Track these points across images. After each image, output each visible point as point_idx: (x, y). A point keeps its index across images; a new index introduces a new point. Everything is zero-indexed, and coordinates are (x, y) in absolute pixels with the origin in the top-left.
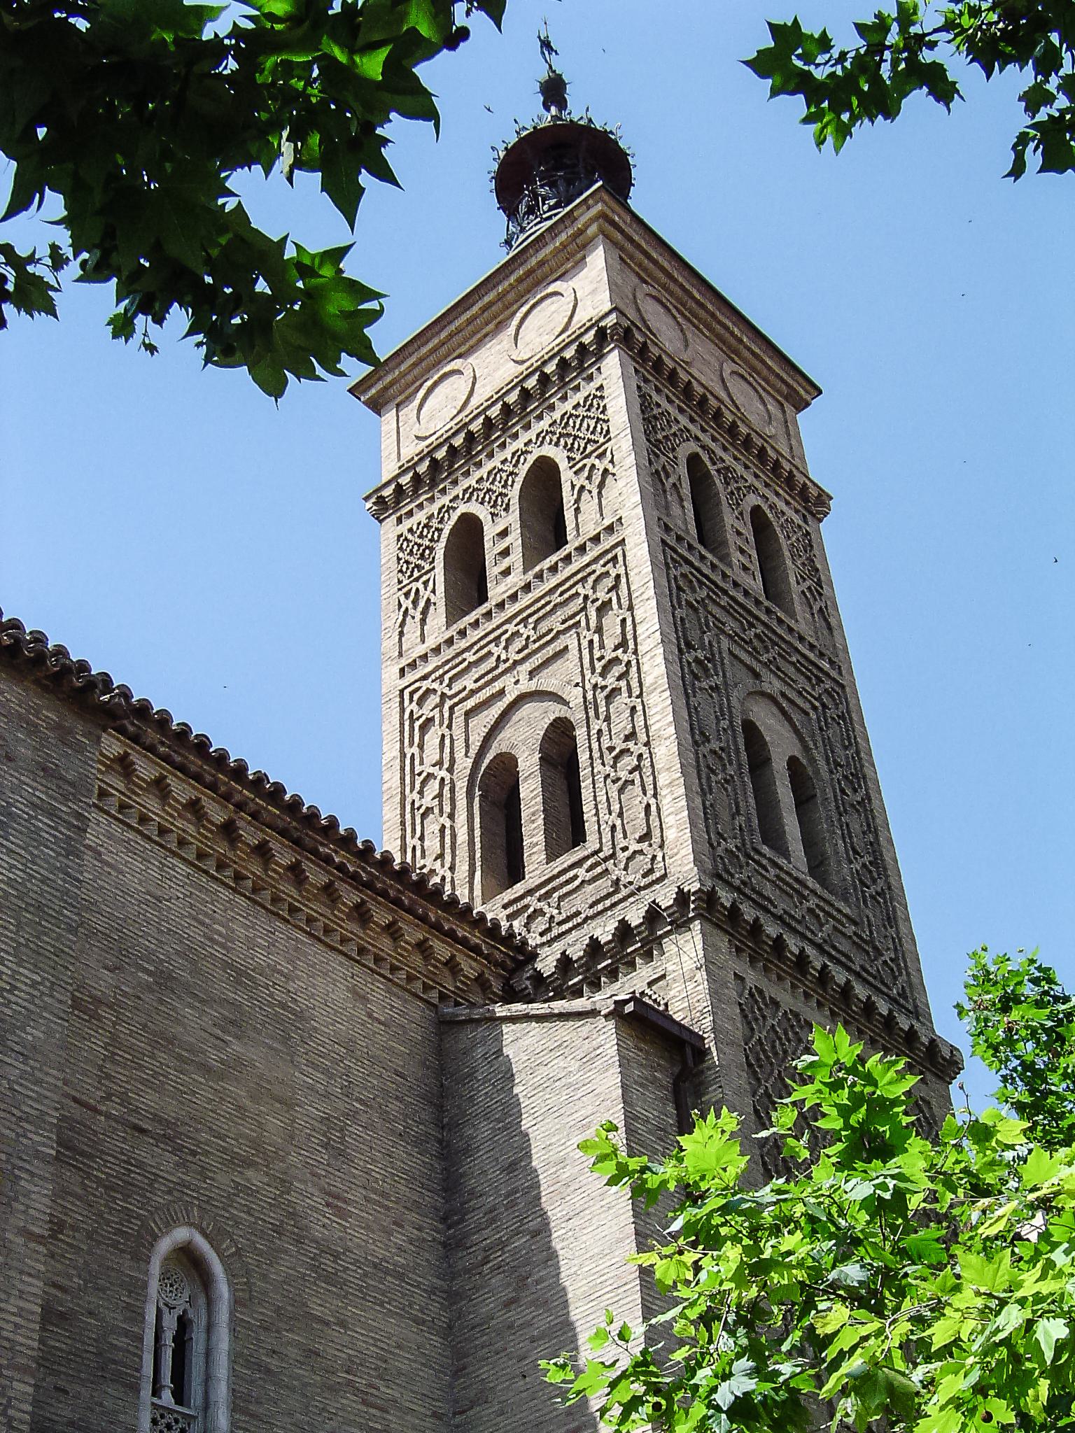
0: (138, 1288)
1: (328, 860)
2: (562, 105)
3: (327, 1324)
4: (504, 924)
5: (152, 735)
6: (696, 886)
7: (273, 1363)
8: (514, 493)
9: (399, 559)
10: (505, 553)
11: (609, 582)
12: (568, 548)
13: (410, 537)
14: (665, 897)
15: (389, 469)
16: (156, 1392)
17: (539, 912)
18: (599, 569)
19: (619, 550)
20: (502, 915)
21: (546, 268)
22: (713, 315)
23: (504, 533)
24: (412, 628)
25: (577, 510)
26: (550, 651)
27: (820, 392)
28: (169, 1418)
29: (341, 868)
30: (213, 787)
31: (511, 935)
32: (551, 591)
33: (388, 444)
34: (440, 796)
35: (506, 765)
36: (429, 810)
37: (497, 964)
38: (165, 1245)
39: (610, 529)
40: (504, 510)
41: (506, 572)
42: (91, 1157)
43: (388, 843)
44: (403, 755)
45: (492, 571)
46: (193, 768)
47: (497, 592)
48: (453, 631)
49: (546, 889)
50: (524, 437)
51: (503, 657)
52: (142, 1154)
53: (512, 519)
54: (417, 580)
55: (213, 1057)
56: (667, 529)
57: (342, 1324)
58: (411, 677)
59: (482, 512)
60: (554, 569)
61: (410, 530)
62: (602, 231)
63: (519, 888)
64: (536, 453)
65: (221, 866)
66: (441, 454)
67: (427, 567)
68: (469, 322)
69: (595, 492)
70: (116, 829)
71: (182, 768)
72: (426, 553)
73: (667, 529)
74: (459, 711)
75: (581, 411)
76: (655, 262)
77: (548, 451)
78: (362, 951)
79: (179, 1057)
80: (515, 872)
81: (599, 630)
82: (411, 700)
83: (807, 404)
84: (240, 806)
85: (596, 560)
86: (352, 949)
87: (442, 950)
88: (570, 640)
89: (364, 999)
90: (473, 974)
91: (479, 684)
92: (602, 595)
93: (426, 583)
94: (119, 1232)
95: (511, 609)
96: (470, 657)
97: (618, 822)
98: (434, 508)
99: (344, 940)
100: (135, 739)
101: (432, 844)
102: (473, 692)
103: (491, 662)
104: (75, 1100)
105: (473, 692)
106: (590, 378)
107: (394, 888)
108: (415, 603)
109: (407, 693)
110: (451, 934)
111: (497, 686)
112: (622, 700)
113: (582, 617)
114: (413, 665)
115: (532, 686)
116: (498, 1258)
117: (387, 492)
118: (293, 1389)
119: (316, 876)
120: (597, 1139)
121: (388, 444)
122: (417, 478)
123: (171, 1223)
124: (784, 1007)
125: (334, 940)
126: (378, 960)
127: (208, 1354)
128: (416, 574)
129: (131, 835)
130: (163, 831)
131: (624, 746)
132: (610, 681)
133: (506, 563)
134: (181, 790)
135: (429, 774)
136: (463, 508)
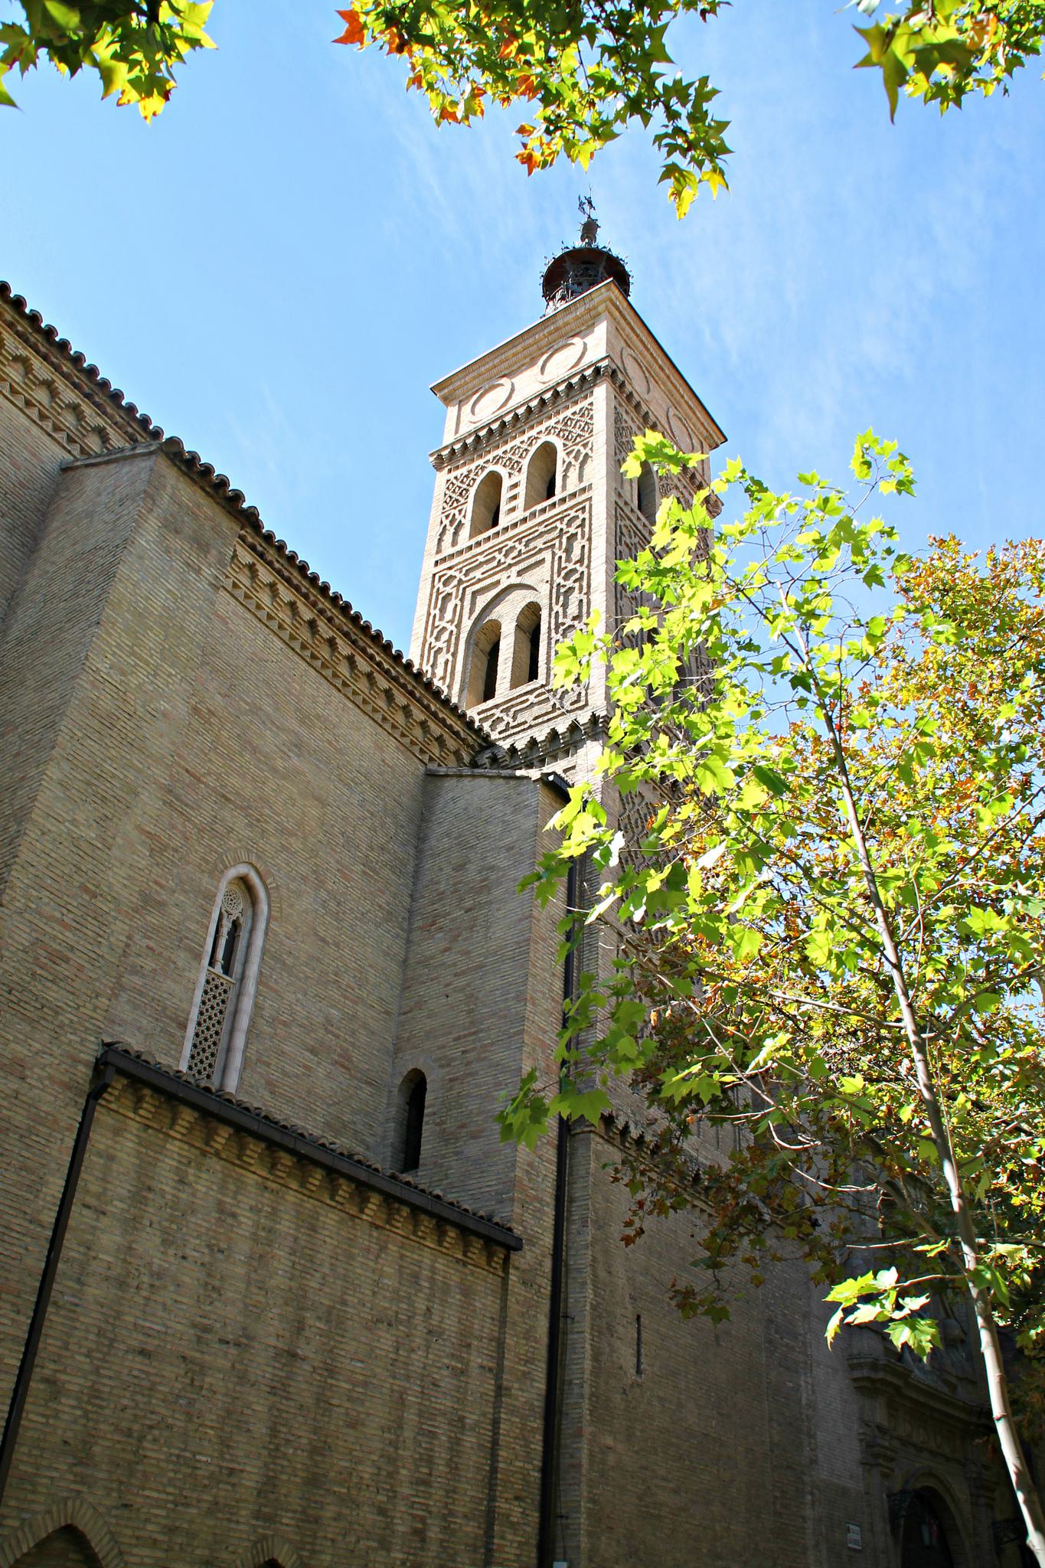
0: (210, 898)
1: (372, 658)
2: (593, 238)
3: (327, 943)
4: (477, 724)
5: (271, 554)
6: (604, 713)
7: (289, 961)
8: (525, 463)
10: (514, 497)
11: (578, 522)
14: (583, 718)
15: (449, 438)
16: (211, 963)
17: (500, 719)
18: (572, 513)
19: (587, 504)
20: (477, 718)
23: (515, 485)
24: (448, 537)
26: (532, 560)
28: (218, 982)
29: (379, 664)
30: (306, 596)
31: (481, 729)
32: (540, 524)
33: (450, 424)
34: (449, 641)
35: (496, 626)
36: (440, 650)
37: (468, 746)
38: (232, 873)
39: (583, 490)
41: (513, 509)
42: (192, 808)
43: (412, 653)
44: (429, 614)
45: (504, 507)
46: (295, 582)
47: (504, 520)
48: (473, 542)
49: (507, 706)
50: (537, 429)
52: (226, 814)
53: (522, 477)
55: (279, 764)
56: (620, 495)
57: (337, 945)
58: (441, 567)
59: (503, 472)
60: (544, 511)
63: (490, 703)
64: (543, 438)
65: (304, 647)
66: (482, 433)
68: (514, 355)
70: (241, 609)
71: (288, 580)
73: (620, 495)
74: (469, 591)
75: (577, 417)
76: (638, 336)
77: (552, 439)
78: (384, 719)
79: (259, 760)
80: (489, 692)
83: (717, 446)
84: (322, 612)
85: (571, 508)
86: (378, 717)
87: (436, 729)
88: (547, 555)
89: (381, 749)
90: (452, 749)
92: (572, 530)
94: (203, 859)
95: (511, 533)
96: (481, 559)
98: (473, 466)
99: (375, 710)
100: (261, 556)
101: (439, 672)
102: (480, 580)
103: (495, 563)
104: (187, 771)
105: (480, 580)
106: (586, 397)
107: (411, 684)
108: (452, 523)
110: (443, 721)
113: (557, 542)
114: (444, 560)
116: (441, 922)
117: (445, 453)
118: (299, 979)
119: (363, 665)
121: (450, 424)
122: (465, 446)
123: (238, 861)
124: (646, 800)
125: (368, 709)
126: (394, 727)
127: (249, 946)
129: (248, 616)
130: (270, 617)
132: (569, 583)
134: (286, 594)
136: (491, 468)
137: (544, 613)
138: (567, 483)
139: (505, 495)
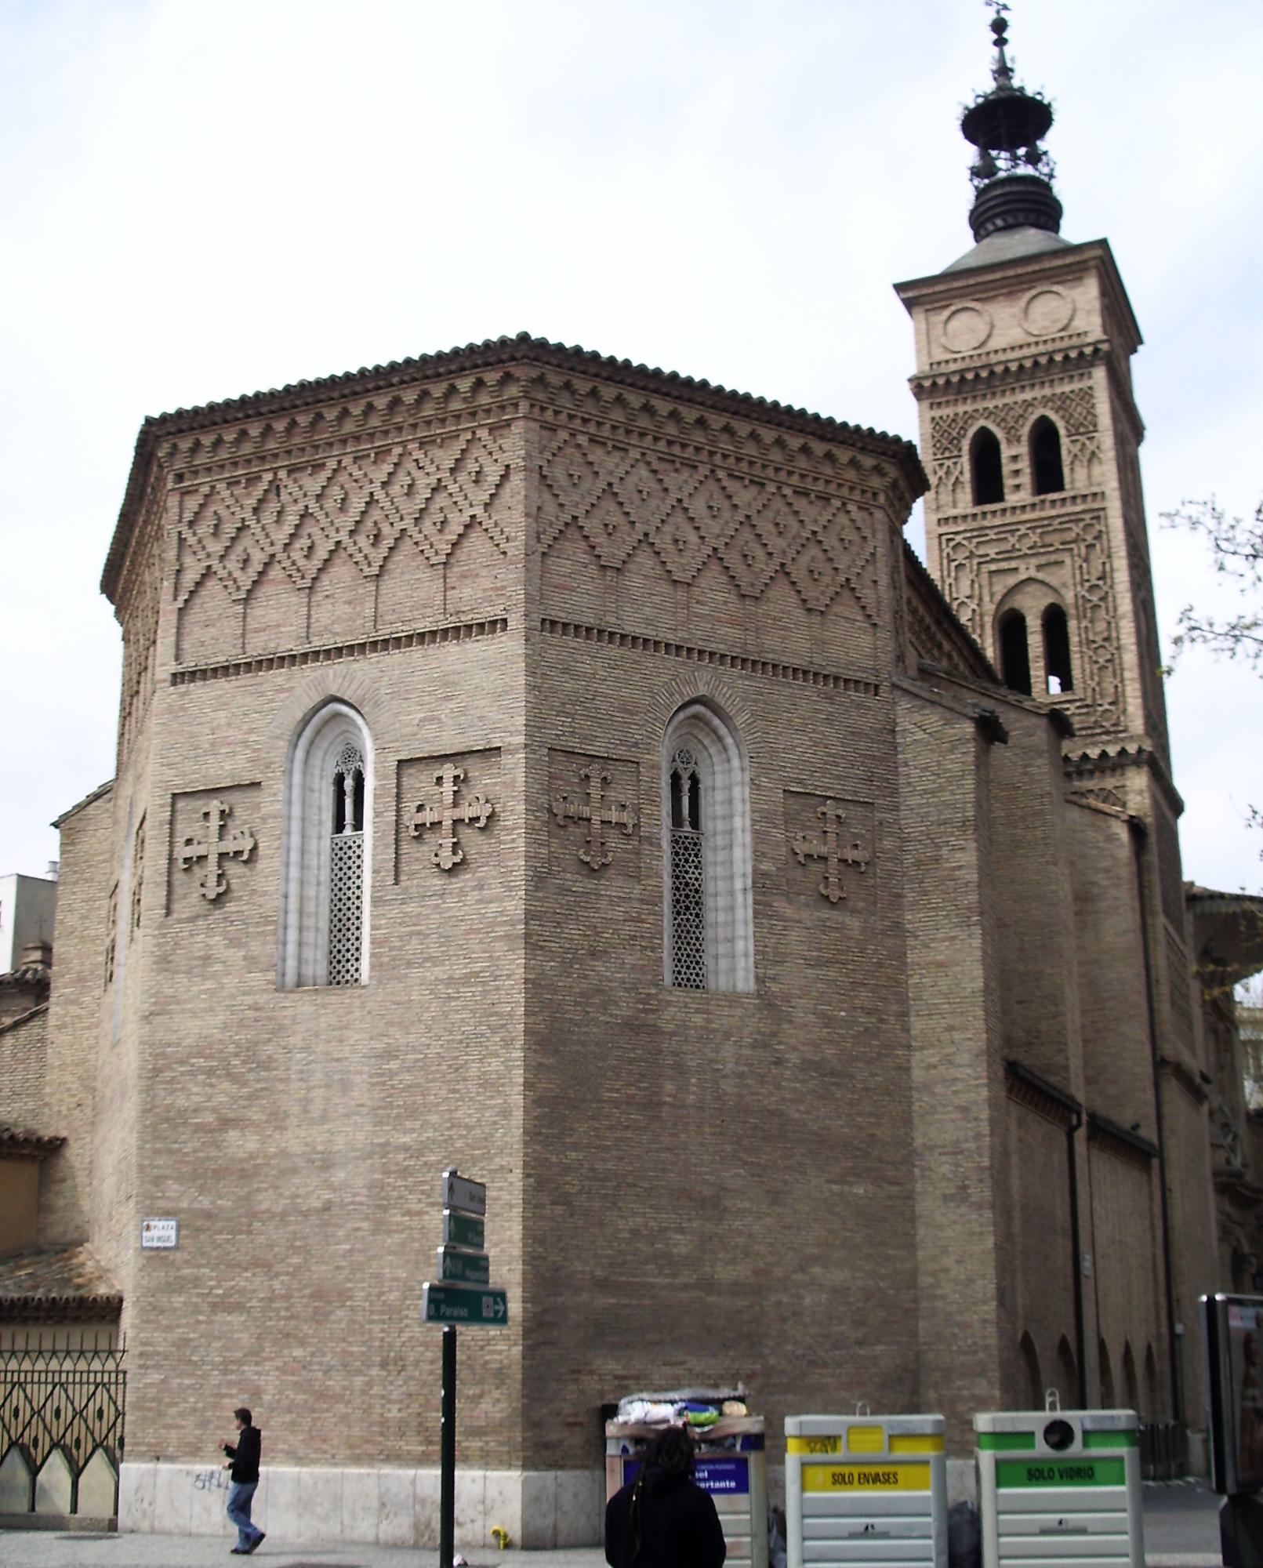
9: (933, 437)
13: (941, 423)
25: (1072, 470)
45: (1009, 482)
51: (1017, 546)
53: (1023, 449)
54: (948, 458)
61: (941, 418)
67: (956, 453)
69: (1086, 464)
72: (955, 441)
81: (1086, 560)
82: (947, 546)
91: (1000, 556)
93: (955, 463)
97: (1097, 688)
109: (944, 538)
111: (1013, 564)
112: (1102, 613)
115: (1040, 576)
120: (1038, 833)
128: (947, 454)
131: (1102, 643)
135: (963, 602)
137: (1072, 625)
138: (1076, 478)
139: (1007, 468)
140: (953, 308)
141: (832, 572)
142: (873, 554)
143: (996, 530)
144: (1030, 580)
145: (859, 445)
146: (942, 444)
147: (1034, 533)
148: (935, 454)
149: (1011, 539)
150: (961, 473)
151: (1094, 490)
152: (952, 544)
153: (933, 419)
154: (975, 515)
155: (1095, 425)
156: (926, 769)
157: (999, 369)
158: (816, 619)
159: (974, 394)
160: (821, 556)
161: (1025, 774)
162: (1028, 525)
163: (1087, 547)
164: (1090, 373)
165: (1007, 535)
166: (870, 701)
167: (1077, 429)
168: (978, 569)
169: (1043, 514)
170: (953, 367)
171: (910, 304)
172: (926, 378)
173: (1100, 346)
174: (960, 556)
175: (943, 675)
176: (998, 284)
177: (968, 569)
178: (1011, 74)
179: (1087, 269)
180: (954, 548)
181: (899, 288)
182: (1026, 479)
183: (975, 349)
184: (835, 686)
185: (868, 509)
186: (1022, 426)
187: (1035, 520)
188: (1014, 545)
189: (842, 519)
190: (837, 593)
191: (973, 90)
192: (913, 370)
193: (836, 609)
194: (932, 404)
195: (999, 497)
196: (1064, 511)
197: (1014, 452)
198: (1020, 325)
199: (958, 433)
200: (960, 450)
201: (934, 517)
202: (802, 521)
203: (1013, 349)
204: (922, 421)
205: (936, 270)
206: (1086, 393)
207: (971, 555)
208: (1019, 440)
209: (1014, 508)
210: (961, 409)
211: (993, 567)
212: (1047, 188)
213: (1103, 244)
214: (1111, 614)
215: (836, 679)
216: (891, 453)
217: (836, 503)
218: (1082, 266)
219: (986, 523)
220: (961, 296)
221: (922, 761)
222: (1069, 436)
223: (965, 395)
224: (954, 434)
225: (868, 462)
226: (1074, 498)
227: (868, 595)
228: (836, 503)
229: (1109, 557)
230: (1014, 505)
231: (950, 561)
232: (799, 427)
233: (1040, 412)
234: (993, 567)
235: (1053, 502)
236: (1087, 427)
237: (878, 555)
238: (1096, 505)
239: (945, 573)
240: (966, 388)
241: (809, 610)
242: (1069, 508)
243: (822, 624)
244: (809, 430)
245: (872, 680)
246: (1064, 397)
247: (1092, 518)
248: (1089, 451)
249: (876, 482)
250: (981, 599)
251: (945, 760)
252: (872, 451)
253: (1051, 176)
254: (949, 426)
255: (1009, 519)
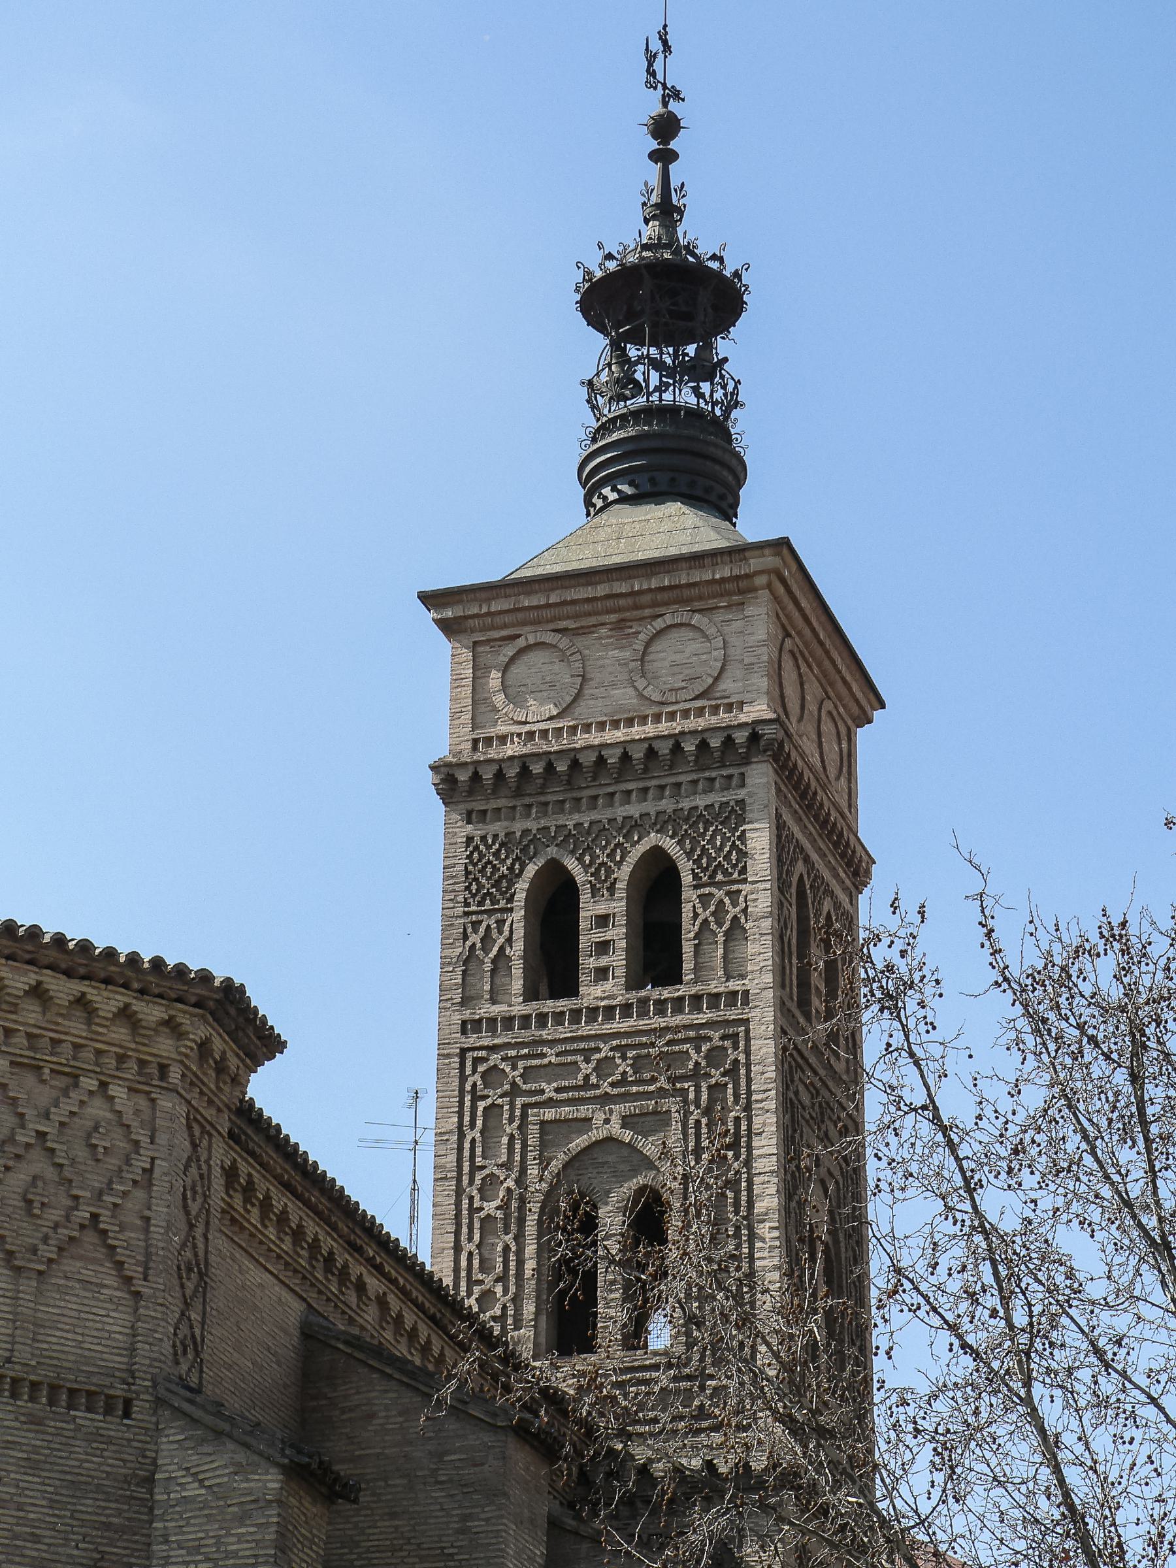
9: (467, 873)
12: (682, 991)
21: (694, 592)
22: (827, 652)
27: (883, 706)
40: (608, 889)
45: (589, 963)
48: (531, 1008)
51: (593, 1080)
53: (618, 906)
54: (489, 912)
62: (769, 586)
67: (502, 904)
82: (474, 1071)
109: (469, 1055)
111: (583, 1111)
128: (488, 905)
133: (603, 961)
139: (588, 937)
140: (521, 642)
141: (69, 1203)
142: (148, 1172)
143: (559, 1048)
144: (610, 1139)
145: (136, 985)
146: (480, 887)
147: (624, 1057)
148: (467, 904)
149: (583, 1065)
150: (509, 940)
151: (734, 985)
152: (481, 1068)
153: (470, 839)
154: (526, 1019)
155: (744, 870)
156: (197, 1550)
157: (588, 759)
158: (28, 1285)
159: (542, 799)
160: (50, 1173)
161: (462, 1531)
162: (614, 1043)
163: (710, 1087)
164: (743, 774)
165: (580, 1058)
166: (112, 1427)
167: (712, 876)
168: (524, 1116)
169: (642, 1024)
170: (511, 750)
171: (448, 627)
172: (464, 765)
173: (760, 730)
174: (494, 1096)
175: (341, 1346)
176: (599, 605)
177: (506, 1116)
178: (676, 216)
179: (754, 590)
180: (484, 1075)
181: (429, 599)
182: (617, 960)
183: (551, 718)
184: (52, 1402)
185: (148, 1093)
186: (619, 864)
187: (627, 1034)
188: (587, 1078)
189: (97, 1110)
190: (71, 1238)
191: (600, 246)
192: (441, 750)
193: (70, 1265)
194: (469, 813)
195: (572, 990)
196: (679, 1020)
197: (601, 909)
198: (632, 683)
199: (511, 869)
200: (511, 900)
201: (457, 1018)
202: (22, 1115)
203: (616, 724)
204: (449, 845)
205: (494, 575)
206: (733, 811)
207: (514, 1091)
208: (612, 889)
209: (593, 1012)
210: (518, 826)
211: (549, 1114)
212: (720, 429)
213: (783, 545)
214: (743, 1212)
215: (54, 1389)
216: (193, 999)
217: (89, 1083)
218: (743, 584)
219: (544, 1034)
220: (536, 622)
221: (191, 1535)
222: (696, 887)
223: (528, 800)
224: (504, 870)
225: (152, 1012)
226: (697, 999)
227: (128, 1240)
228: (89, 1083)
229: (748, 1108)
230: (594, 1004)
231: (475, 1098)
232: (27, 956)
233: (652, 839)
234: (549, 1114)
235: (661, 1005)
236: (726, 873)
237: (157, 1173)
238: (732, 1014)
239: (467, 1119)
240: (530, 789)
241: (18, 1269)
242: (687, 1017)
243: (39, 1292)
244: (46, 961)
245: (119, 1390)
246: (694, 817)
247: (723, 1038)
248: (729, 917)
249: (165, 1047)
250: (523, 1171)
251: (228, 1535)
252: (161, 996)
253: (732, 403)
254: (497, 854)
255: (585, 1030)
